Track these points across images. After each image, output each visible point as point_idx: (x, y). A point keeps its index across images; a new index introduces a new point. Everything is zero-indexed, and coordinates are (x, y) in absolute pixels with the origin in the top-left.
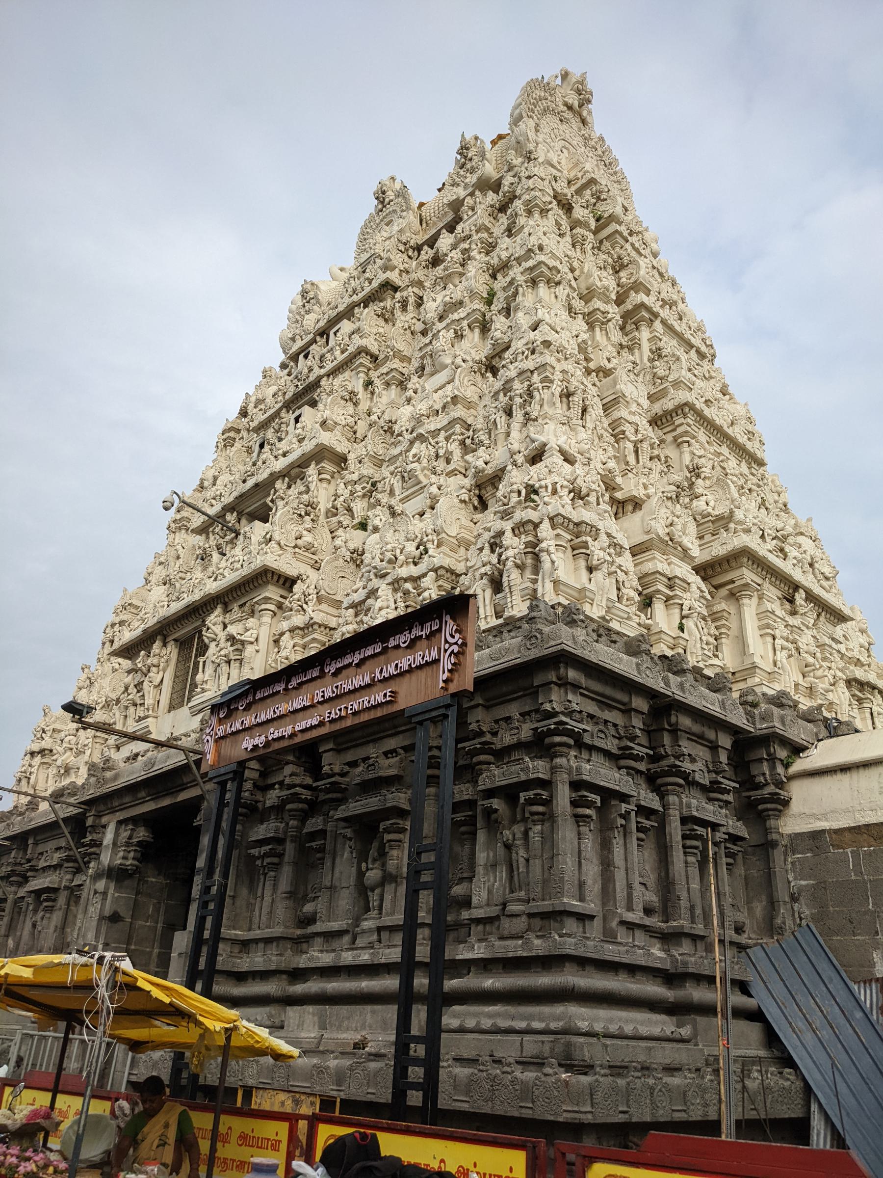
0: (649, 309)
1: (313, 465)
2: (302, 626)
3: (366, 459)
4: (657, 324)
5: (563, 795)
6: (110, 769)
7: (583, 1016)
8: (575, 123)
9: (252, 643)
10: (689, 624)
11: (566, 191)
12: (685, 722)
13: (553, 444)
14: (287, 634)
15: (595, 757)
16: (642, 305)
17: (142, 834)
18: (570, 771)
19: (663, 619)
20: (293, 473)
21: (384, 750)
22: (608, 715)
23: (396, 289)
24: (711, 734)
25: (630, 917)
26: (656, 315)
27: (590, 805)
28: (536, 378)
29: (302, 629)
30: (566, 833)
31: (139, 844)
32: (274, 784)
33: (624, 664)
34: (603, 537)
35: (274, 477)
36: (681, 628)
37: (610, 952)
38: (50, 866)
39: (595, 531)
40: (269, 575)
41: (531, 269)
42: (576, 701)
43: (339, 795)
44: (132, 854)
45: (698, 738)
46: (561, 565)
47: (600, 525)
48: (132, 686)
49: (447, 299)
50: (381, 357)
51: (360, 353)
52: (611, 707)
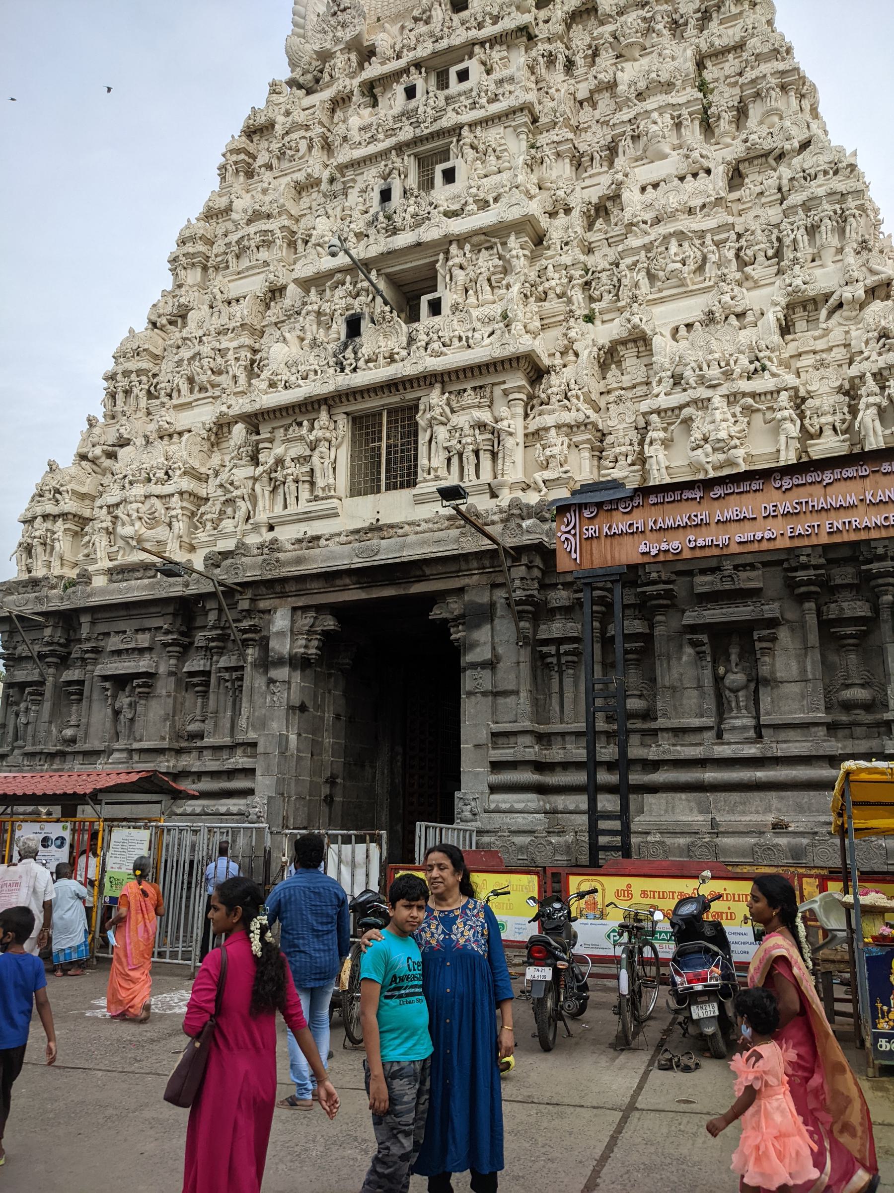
1: (512, 237)
2: (573, 423)
3: (575, 243)
6: (279, 550)
9: (511, 434)
14: (553, 431)
17: (329, 623)
20: (475, 239)
21: (736, 563)
29: (571, 427)
31: (324, 633)
32: (557, 584)
35: (448, 241)
40: (522, 362)
43: (669, 602)
44: (315, 643)
48: (288, 459)
49: (654, 75)
50: (543, 120)
51: (522, 110)
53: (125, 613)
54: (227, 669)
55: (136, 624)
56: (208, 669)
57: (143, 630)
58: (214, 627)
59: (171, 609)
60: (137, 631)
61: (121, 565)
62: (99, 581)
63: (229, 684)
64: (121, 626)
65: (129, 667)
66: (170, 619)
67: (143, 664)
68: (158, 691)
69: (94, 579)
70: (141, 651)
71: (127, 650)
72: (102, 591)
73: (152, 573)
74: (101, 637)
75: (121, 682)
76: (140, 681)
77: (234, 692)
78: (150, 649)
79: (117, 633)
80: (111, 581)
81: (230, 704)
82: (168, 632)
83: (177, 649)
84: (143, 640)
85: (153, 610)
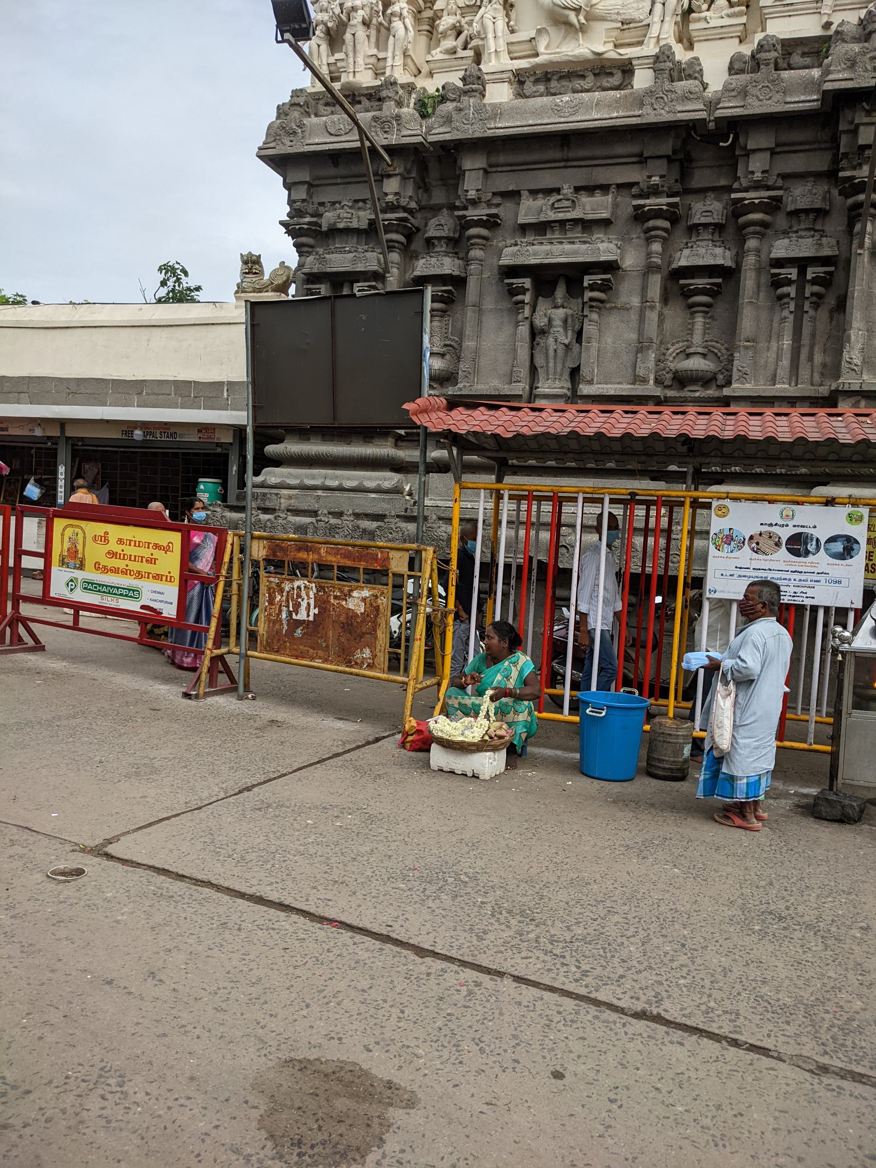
38: (576, 221)
53: (558, 155)
54: (779, 263)
55: (580, 176)
56: (729, 263)
57: (590, 189)
58: (757, 186)
59: (666, 148)
60: (577, 189)
61: (552, 63)
62: (499, 94)
63: (792, 290)
64: (547, 179)
65: (575, 253)
66: (661, 166)
67: (603, 248)
68: (623, 299)
69: (488, 87)
70: (587, 225)
71: (562, 223)
72: (497, 112)
73: (616, 80)
74: (497, 200)
75: (547, 279)
76: (598, 278)
77: (799, 308)
78: (606, 223)
79: (534, 192)
80: (520, 95)
81: (789, 326)
82: (654, 191)
83: (666, 224)
84: (595, 206)
85: (620, 150)
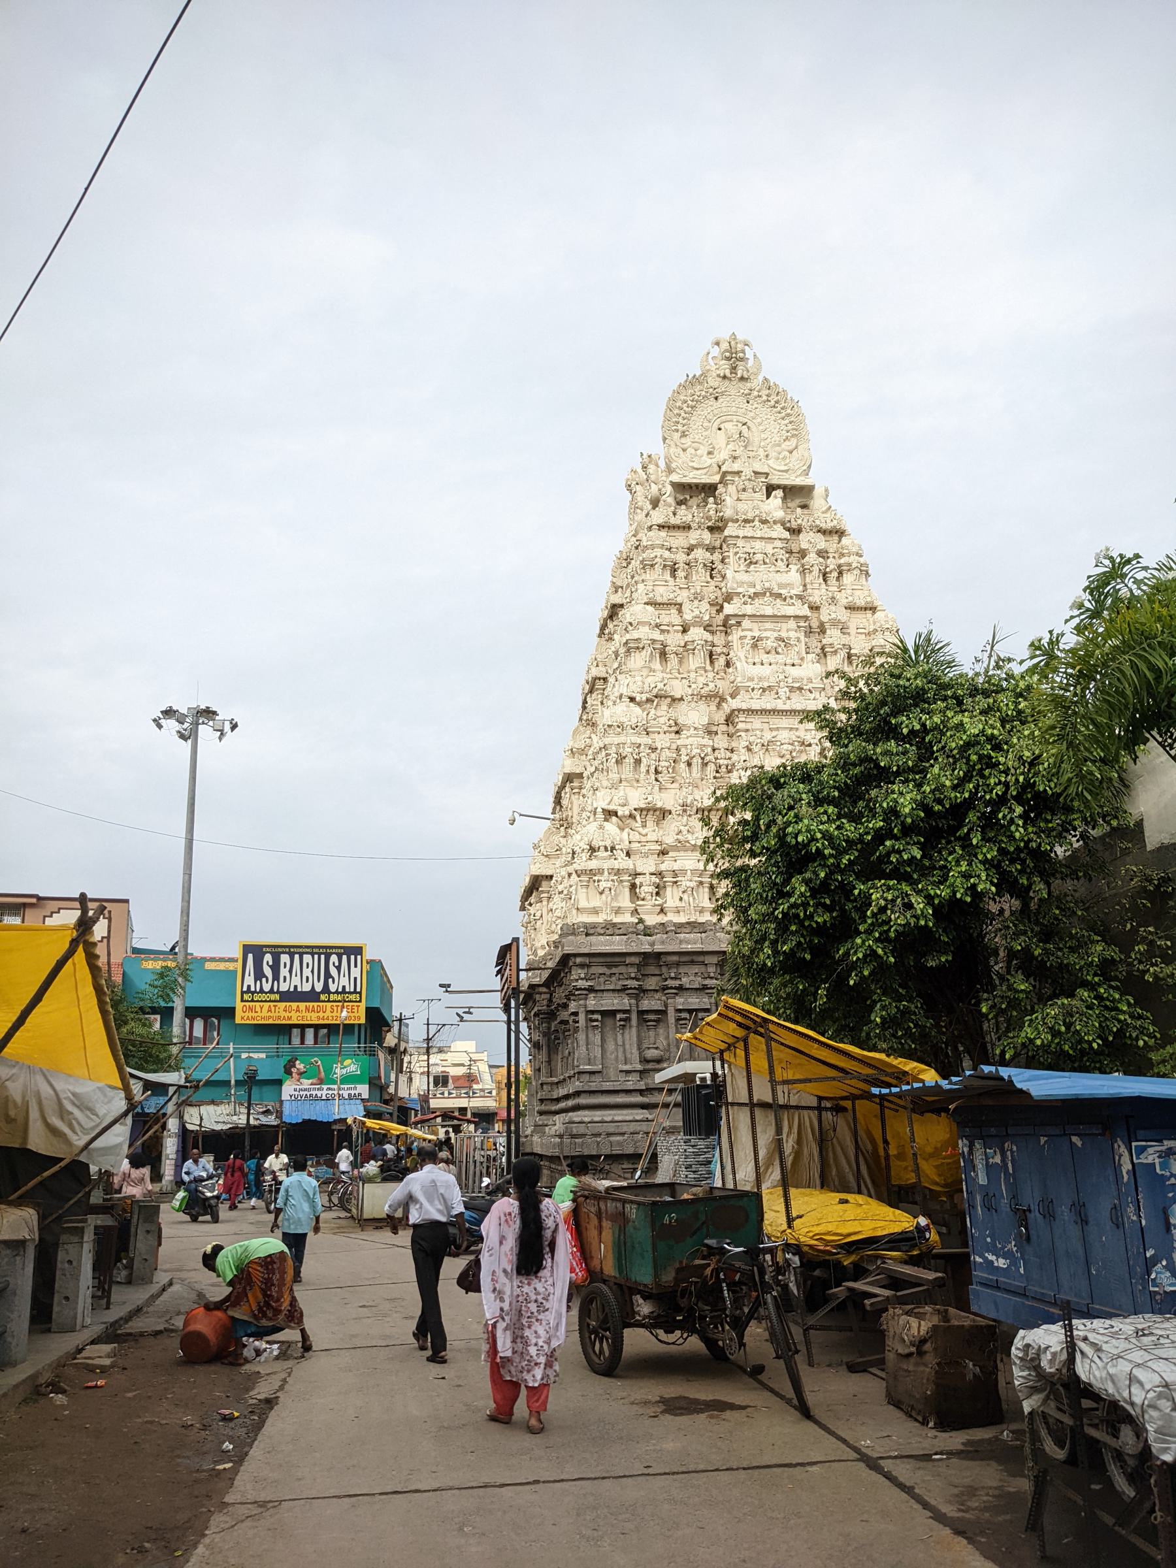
0: (736, 615)
4: (746, 623)
5: (582, 1018)
7: (576, 1116)
8: (734, 388)
10: (685, 897)
11: (684, 519)
12: (675, 958)
13: (599, 810)
15: (605, 994)
16: (728, 617)
18: (585, 1006)
19: (671, 898)
22: (614, 970)
23: (622, 606)
24: (701, 958)
25: (627, 1067)
26: (744, 616)
27: (597, 1020)
28: (604, 753)
30: (581, 1036)
33: (616, 944)
34: (606, 873)
36: (681, 899)
37: (607, 1086)
39: (600, 871)
41: (626, 643)
42: (582, 973)
45: (692, 962)
46: (584, 899)
47: (605, 866)
52: (616, 966)
